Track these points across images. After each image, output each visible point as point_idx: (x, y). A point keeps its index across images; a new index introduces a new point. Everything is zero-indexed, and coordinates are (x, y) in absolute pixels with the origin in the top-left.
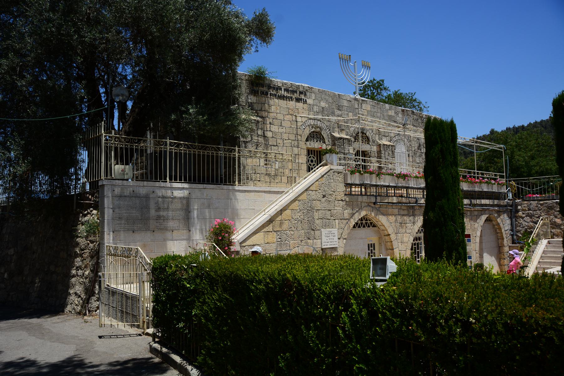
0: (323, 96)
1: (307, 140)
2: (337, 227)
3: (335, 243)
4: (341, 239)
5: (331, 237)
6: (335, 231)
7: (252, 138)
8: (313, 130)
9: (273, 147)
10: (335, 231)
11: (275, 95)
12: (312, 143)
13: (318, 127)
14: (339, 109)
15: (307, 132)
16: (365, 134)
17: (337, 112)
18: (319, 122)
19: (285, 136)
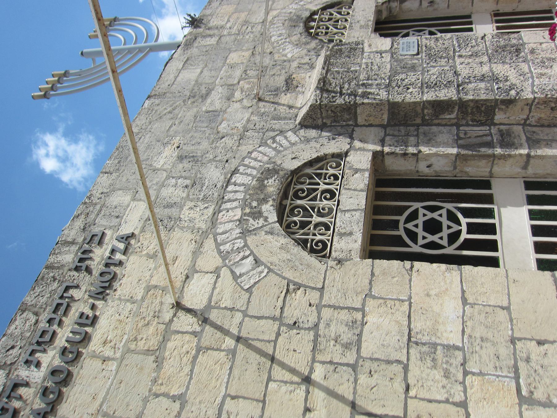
1: (320, 250)
8: (269, 211)
12: (342, 221)
13: (261, 187)
14: (204, 97)
15: (275, 246)
16: (314, 13)
17: (215, 100)
18: (238, 178)
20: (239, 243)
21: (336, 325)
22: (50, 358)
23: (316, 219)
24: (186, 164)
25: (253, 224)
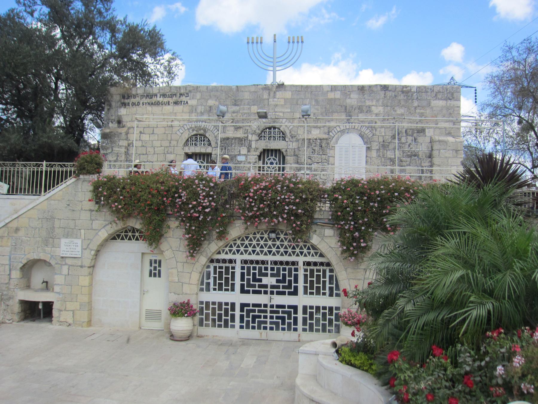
0: (212, 94)
1: (186, 144)
2: (83, 237)
3: (77, 253)
4: (88, 250)
5: (72, 247)
6: (79, 242)
7: (112, 150)
8: (195, 132)
9: (141, 156)
10: (79, 242)
11: (149, 104)
15: (186, 136)
19: (157, 144)
20: (186, 128)
21: (171, 149)
22: (161, 99)
23: (194, 143)
24: (208, 109)
25: (191, 131)
